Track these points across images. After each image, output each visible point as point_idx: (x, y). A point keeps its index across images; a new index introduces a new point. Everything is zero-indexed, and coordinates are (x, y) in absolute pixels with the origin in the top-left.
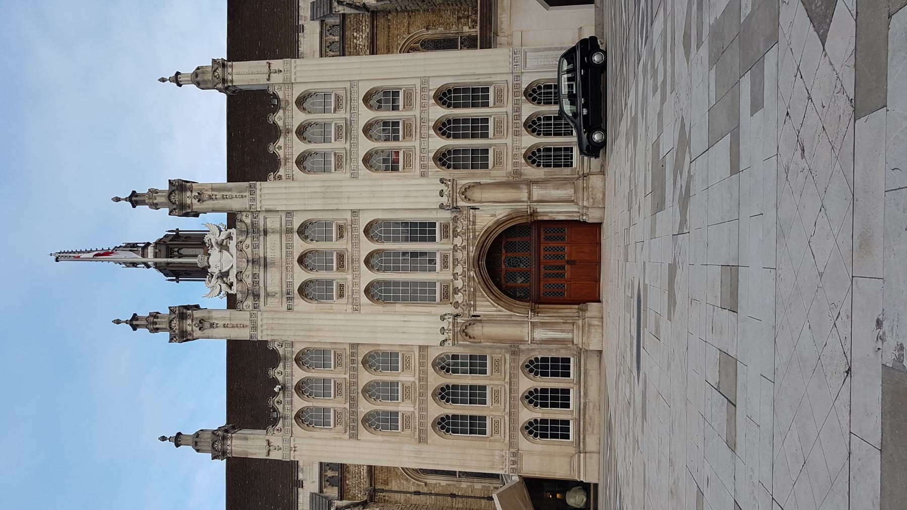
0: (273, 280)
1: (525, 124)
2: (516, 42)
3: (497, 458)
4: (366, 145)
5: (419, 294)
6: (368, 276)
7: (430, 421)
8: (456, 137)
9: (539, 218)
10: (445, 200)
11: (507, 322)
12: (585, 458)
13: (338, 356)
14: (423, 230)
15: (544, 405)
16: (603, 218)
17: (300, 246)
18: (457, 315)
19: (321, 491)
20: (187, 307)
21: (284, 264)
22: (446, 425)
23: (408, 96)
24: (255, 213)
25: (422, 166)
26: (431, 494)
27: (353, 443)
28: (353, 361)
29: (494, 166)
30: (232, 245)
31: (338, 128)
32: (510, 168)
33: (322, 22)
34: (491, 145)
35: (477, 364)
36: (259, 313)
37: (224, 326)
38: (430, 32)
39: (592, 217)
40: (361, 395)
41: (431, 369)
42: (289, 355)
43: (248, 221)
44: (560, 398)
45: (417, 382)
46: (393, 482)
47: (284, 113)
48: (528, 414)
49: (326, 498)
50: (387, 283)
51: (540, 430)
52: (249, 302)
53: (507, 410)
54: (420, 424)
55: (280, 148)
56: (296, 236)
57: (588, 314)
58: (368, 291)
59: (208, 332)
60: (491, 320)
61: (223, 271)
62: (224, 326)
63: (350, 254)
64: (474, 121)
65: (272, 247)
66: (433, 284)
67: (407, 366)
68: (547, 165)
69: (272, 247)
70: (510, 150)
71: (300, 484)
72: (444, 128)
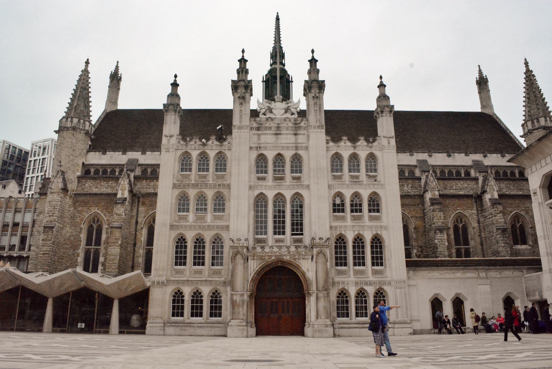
0: (267, 138)
1: (362, 288)
2: (412, 282)
3: (161, 273)
4: (348, 194)
5: (259, 226)
6: (270, 195)
7: (183, 232)
8: (354, 247)
9: (307, 298)
10: (317, 241)
11: (245, 279)
12: (160, 326)
13: (223, 177)
14: (298, 227)
15: (193, 301)
16: (308, 337)
17: (288, 155)
18: (248, 248)
19: (140, 165)
20: (251, 90)
21: (277, 145)
22: (181, 243)
23: (378, 219)
24: (307, 128)
25: (336, 227)
26: (136, 231)
27: (171, 186)
28: (219, 185)
29: (337, 270)
30: (288, 115)
31: (357, 177)
32: (337, 279)
33: (416, 166)
34: (349, 268)
35: (216, 260)
36: (248, 131)
37: (241, 111)
38: (413, 230)
39: (308, 330)
40: (199, 190)
41: (214, 232)
42: (223, 147)
44: (197, 311)
45: (207, 224)
46: (144, 208)
47: (365, 146)
48: (187, 292)
49: (135, 168)
50: (266, 206)
51: (178, 298)
52: (255, 125)
53: (190, 279)
54: (182, 226)
55: (345, 143)
56: (293, 152)
57: (249, 329)
59: (238, 101)
60: (246, 268)
61: (273, 111)
62: (241, 111)
63: (284, 184)
64: (363, 258)
65: (287, 139)
66: (266, 233)
67: (216, 218)
68: (338, 302)
69: (287, 139)
70: (346, 279)
71: (144, 153)
72: (359, 241)
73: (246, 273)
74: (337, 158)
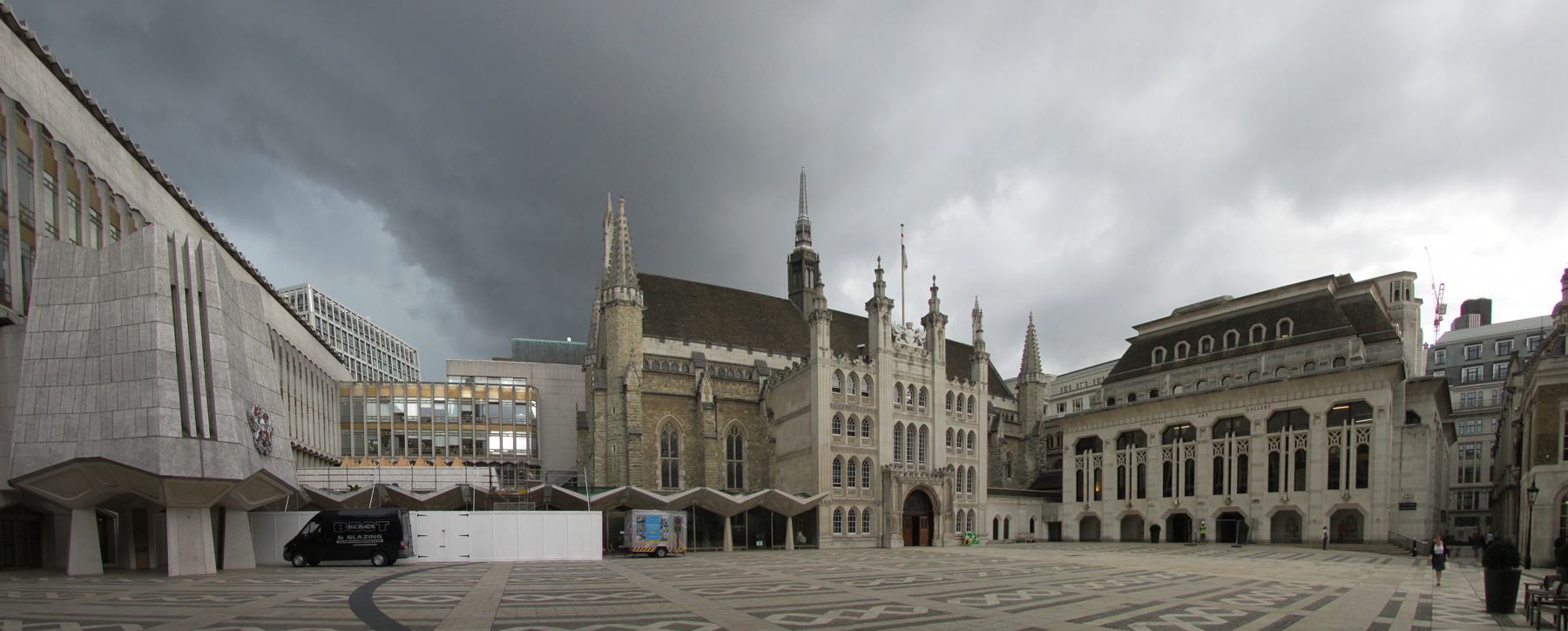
22: (837, 463)
39: (936, 541)
51: (838, 515)
60: (900, 491)
73: (898, 496)
74: (949, 396)
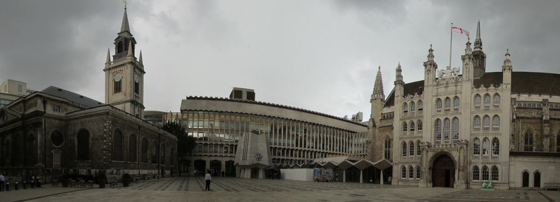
6: (442, 119)
17: (452, 97)
24: (461, 82)
39: (455, 186)
43: (460, 80)
58: (438, 120)
65: (452, 88)
69: (452, 88)
